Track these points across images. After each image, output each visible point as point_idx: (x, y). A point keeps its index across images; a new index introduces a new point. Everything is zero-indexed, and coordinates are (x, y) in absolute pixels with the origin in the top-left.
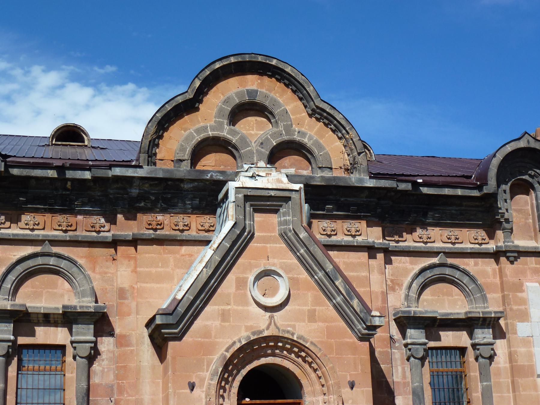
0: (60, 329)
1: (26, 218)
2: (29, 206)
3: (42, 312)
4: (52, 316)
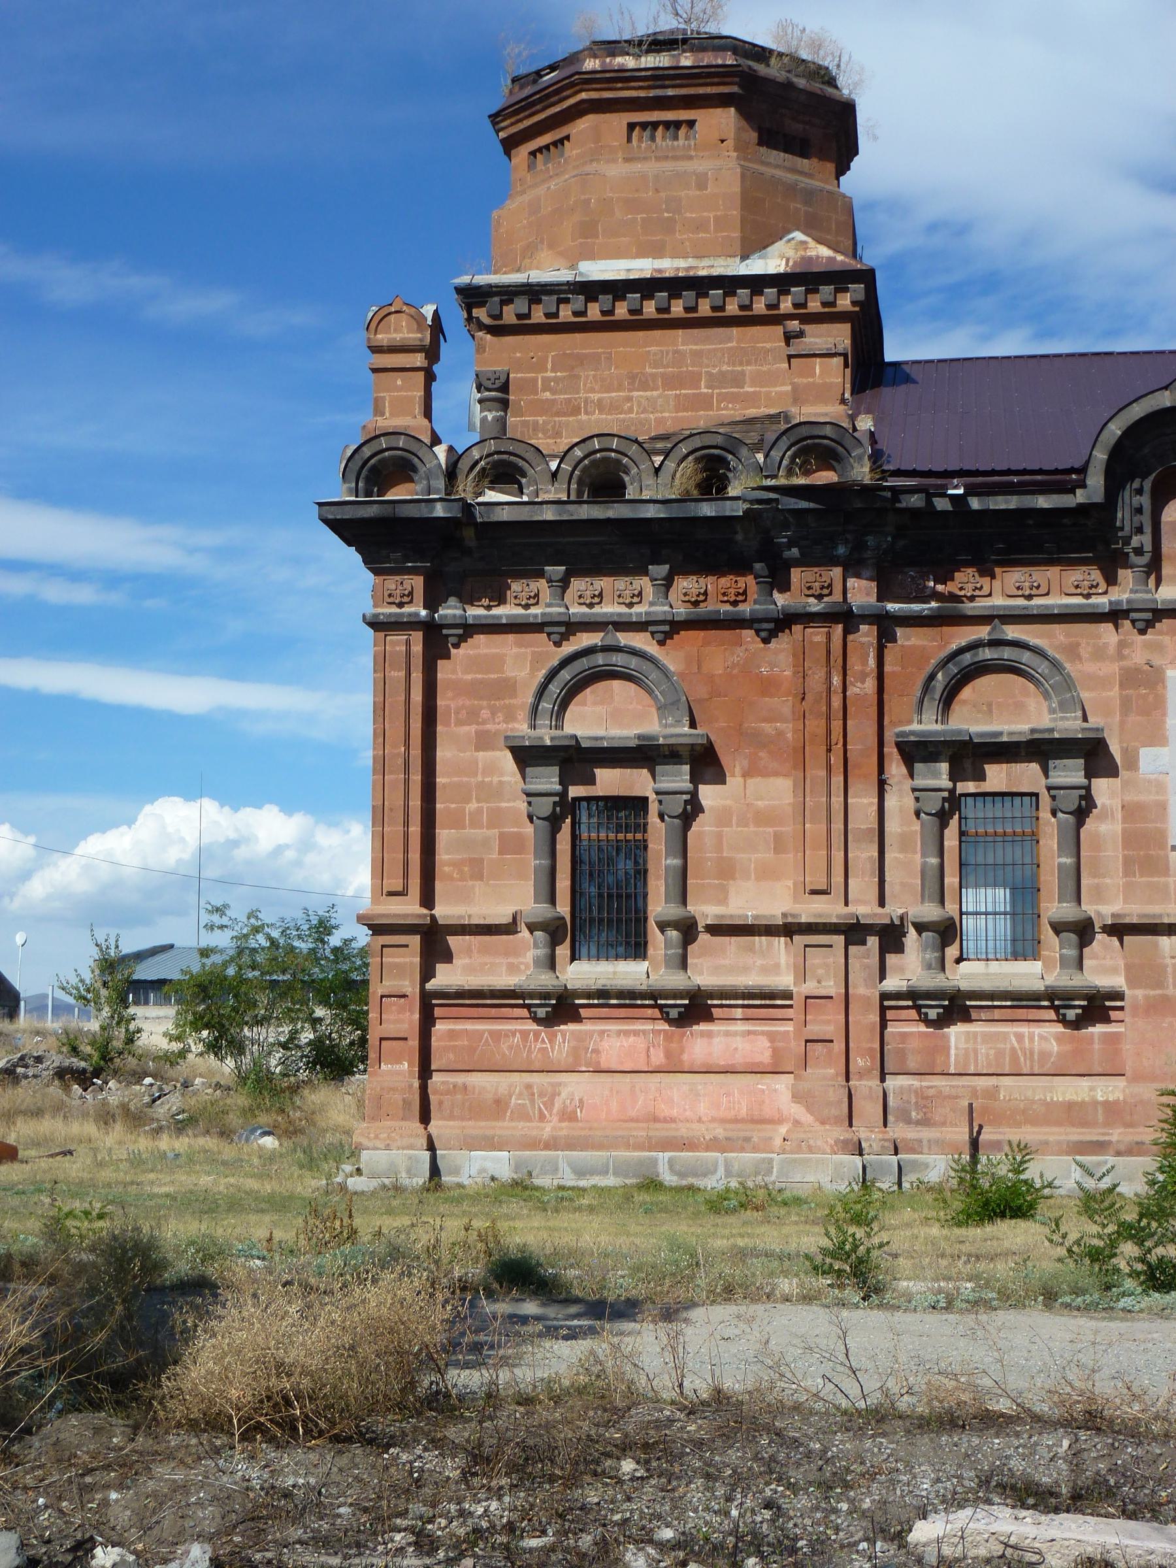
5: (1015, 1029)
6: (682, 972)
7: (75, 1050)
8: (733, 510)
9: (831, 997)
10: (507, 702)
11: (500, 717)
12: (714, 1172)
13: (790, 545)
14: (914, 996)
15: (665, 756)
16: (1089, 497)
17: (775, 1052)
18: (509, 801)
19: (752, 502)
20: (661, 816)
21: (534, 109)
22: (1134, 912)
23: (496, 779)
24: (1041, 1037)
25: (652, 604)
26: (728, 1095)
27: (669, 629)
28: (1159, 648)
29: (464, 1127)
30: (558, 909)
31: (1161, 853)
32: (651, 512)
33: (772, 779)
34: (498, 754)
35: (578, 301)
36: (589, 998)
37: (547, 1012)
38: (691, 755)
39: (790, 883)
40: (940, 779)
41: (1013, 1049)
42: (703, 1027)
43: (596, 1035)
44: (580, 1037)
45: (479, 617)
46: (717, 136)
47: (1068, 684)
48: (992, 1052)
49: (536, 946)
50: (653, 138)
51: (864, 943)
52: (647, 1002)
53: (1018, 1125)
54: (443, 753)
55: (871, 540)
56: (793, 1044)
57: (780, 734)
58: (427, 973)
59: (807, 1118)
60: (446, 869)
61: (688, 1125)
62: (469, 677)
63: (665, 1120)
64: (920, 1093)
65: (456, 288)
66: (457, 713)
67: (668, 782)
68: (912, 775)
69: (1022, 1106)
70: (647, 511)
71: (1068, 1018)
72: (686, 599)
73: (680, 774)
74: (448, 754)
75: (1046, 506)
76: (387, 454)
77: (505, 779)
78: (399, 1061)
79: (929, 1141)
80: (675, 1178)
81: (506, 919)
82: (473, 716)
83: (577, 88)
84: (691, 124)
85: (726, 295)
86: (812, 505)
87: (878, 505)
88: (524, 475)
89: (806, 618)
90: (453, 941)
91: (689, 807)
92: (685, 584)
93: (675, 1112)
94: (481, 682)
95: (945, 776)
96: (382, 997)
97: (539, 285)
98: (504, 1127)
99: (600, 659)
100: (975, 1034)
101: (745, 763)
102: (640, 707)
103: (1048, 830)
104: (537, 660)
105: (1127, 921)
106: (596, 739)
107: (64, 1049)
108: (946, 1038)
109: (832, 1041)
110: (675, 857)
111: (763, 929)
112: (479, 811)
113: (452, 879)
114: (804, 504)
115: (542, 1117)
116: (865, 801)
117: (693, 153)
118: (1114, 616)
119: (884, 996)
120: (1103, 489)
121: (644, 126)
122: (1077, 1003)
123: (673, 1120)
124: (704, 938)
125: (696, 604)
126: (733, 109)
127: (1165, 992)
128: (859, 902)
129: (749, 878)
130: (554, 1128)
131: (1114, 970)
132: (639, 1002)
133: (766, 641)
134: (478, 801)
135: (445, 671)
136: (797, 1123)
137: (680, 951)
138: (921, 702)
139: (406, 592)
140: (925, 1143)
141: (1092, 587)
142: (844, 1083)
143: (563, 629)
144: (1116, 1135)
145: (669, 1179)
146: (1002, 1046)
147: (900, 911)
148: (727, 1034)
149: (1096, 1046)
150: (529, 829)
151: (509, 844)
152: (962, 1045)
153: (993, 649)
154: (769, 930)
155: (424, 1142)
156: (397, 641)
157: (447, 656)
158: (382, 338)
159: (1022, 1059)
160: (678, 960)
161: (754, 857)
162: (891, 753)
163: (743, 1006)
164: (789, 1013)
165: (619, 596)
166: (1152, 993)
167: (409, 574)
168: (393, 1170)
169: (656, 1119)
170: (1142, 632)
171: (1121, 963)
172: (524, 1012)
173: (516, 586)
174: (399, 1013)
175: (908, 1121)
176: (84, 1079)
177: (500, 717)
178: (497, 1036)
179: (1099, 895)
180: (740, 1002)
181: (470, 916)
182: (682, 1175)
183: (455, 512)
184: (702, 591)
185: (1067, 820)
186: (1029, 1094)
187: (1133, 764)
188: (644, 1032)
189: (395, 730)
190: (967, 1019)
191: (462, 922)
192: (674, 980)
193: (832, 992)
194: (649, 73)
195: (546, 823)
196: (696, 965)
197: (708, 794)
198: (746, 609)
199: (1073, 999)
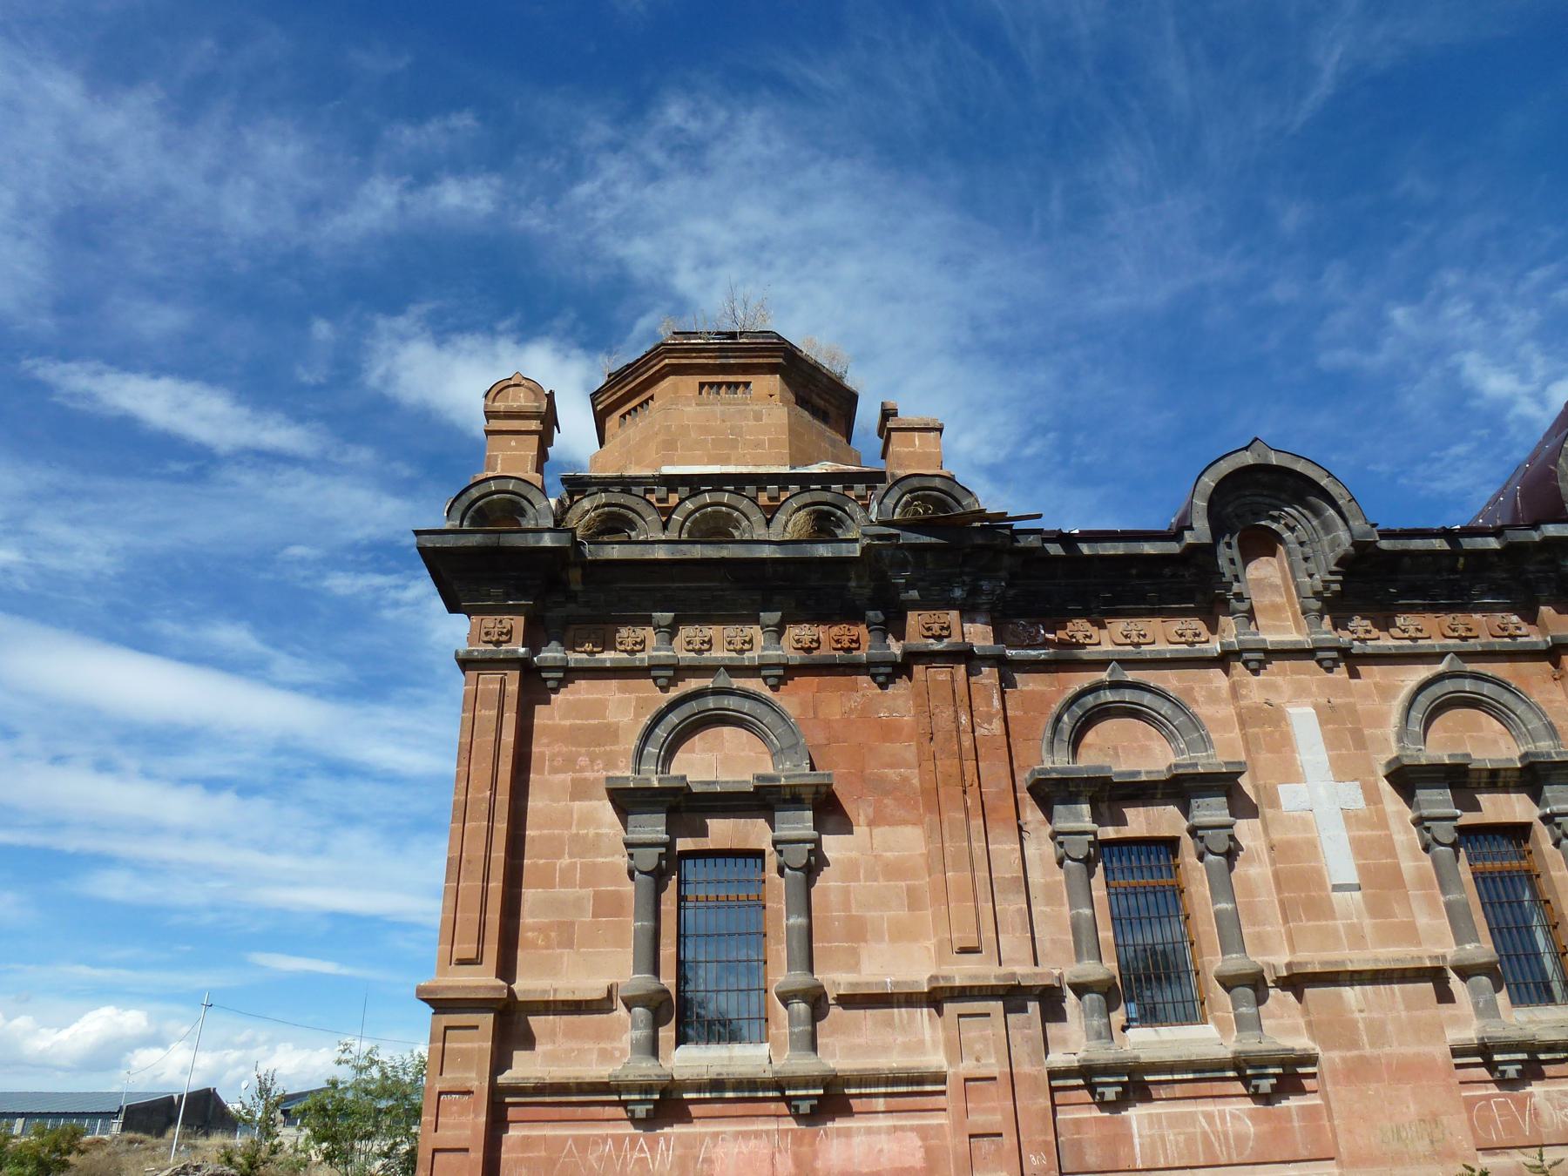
0: (1513, 796)
1: (1400, 621)
2: (1401, 602)
3: (1489, 767)
4: (1503, 773)
5: (1200, 1108)
8: (849, 552)
9: (994, 1079)
10: (608, 748)
11: (600, 764)
13: (909, 586)
14: (1088, 1074)
15: (785, 801)
16: (1198, 539)
17: (929, 1152)
18: (606, 856)
19: (873, 537)
20: (781, 872)
21: (627, 380)
22: (1314, 959)
23: (592, 832)
24: (1233, 1116)
25: (764, 649)
27: (787, 673)
28: (1273, 687)
30: (662, 982)
32: (767, 552)
33: (900, 829)
34: (595, 803)
35: (661, 491)
36: (699, 1091)
39: (931, 943)
40: (1083, 821)
41: (1205, 1135)
42: (839, 1123)
44: (684, 1141)
45: (581, 659)
46: (766, 392)
47: (1195, 722)
48: (1182, 1138)
49: (635, 1026)
50: (718, 393)
51: (1024, 1009)
52: (770, 1094)
54: (536, 803)
55: (985, 585)
56: (950, 1141)
57: (905, 780)
58: (500, 1062)
60: (530, 934)
62: (567, 723)
65: (562, 479)
67: (790, 829)
68: (1049, 817)
70: (762, 552)
71: (1261, 1091)
72: (799, 646)
73: (803, 821)
74: (540, 804)
75: (1152, 552)
76: (495, 496)
77: (603, 831)
81: (599, 994)
82: (569, 763)
83: (662, 356)
84: (747, 385)
85: (780, 489)
86: (933, 540)
87: (998, 541)
88: (633, 530)
89: (929, 657)
90: (536, 1022)
91: (813, 858)
92: (797, 631)
94: (580, 728)
95: (1088, 819)
96: (440, 1093)
97: (630, 477)
99: (711, 702)
100: (1159, 1116)
101: (870, 811)
102: (752, 754)
103: (1197, 875)
104: (641, 705)
105: (1309, 969)
108: (1126, 1123)
109: (1000, 1135)
110: (799, 916)
111: (902, 999)
116: (1007, 847)
117: (749, 402)
118: (1223, 660)
119: (1053, 1074)
120: (1209, 532)
121: (711, 385)
122: (1271, 1071)
124: (835, 1011)
125: (809, 650)
126: (778, 376)
127: (1362, 1052)
131: (1295, 1030)
132: (760, 1094)
133: (883, 686)
134: (571, 856)
137: (809, 1028)
138: (1052, 743)
139: (505, 630)
141: (1196, 635)
143: (671, 673)
146: (1193, 1130)
147: (1056, 972)
148: (869, 1131)
150: (629, 888)
151: (606, 905)
152: (1146, 1132)
153: (1113, 692)
154: (909, 1000)
157: (548, 702)
158: (500, 405)
159: (1217, 1145)
160: (807, 1039)
161: (886, 914)
162: (1024, 798)
163: (886, 1095)
165: (730, 643)
167: (509, 614)
170: (1255, 672)
171: (1302, 1022)
172: (620, 1112)
174: (461, 1115)
177: (600, 764)
178: (583, 1144)
179: (1262, 943)
180: (882, 1090)
181: (555, 991)
183: (562, 541)
184: (815, 638)
185: (1219, 862)
187: (1274, 803)
188: (767, 1132)
189: (482, 771)
190: (1147, 1098)
191: (546, 998)
193: (995, 1072)
195: (650, 878)
196: (826, 1045)
197: (832, 845)
198: (862, 655)
199: (1266, 1067)
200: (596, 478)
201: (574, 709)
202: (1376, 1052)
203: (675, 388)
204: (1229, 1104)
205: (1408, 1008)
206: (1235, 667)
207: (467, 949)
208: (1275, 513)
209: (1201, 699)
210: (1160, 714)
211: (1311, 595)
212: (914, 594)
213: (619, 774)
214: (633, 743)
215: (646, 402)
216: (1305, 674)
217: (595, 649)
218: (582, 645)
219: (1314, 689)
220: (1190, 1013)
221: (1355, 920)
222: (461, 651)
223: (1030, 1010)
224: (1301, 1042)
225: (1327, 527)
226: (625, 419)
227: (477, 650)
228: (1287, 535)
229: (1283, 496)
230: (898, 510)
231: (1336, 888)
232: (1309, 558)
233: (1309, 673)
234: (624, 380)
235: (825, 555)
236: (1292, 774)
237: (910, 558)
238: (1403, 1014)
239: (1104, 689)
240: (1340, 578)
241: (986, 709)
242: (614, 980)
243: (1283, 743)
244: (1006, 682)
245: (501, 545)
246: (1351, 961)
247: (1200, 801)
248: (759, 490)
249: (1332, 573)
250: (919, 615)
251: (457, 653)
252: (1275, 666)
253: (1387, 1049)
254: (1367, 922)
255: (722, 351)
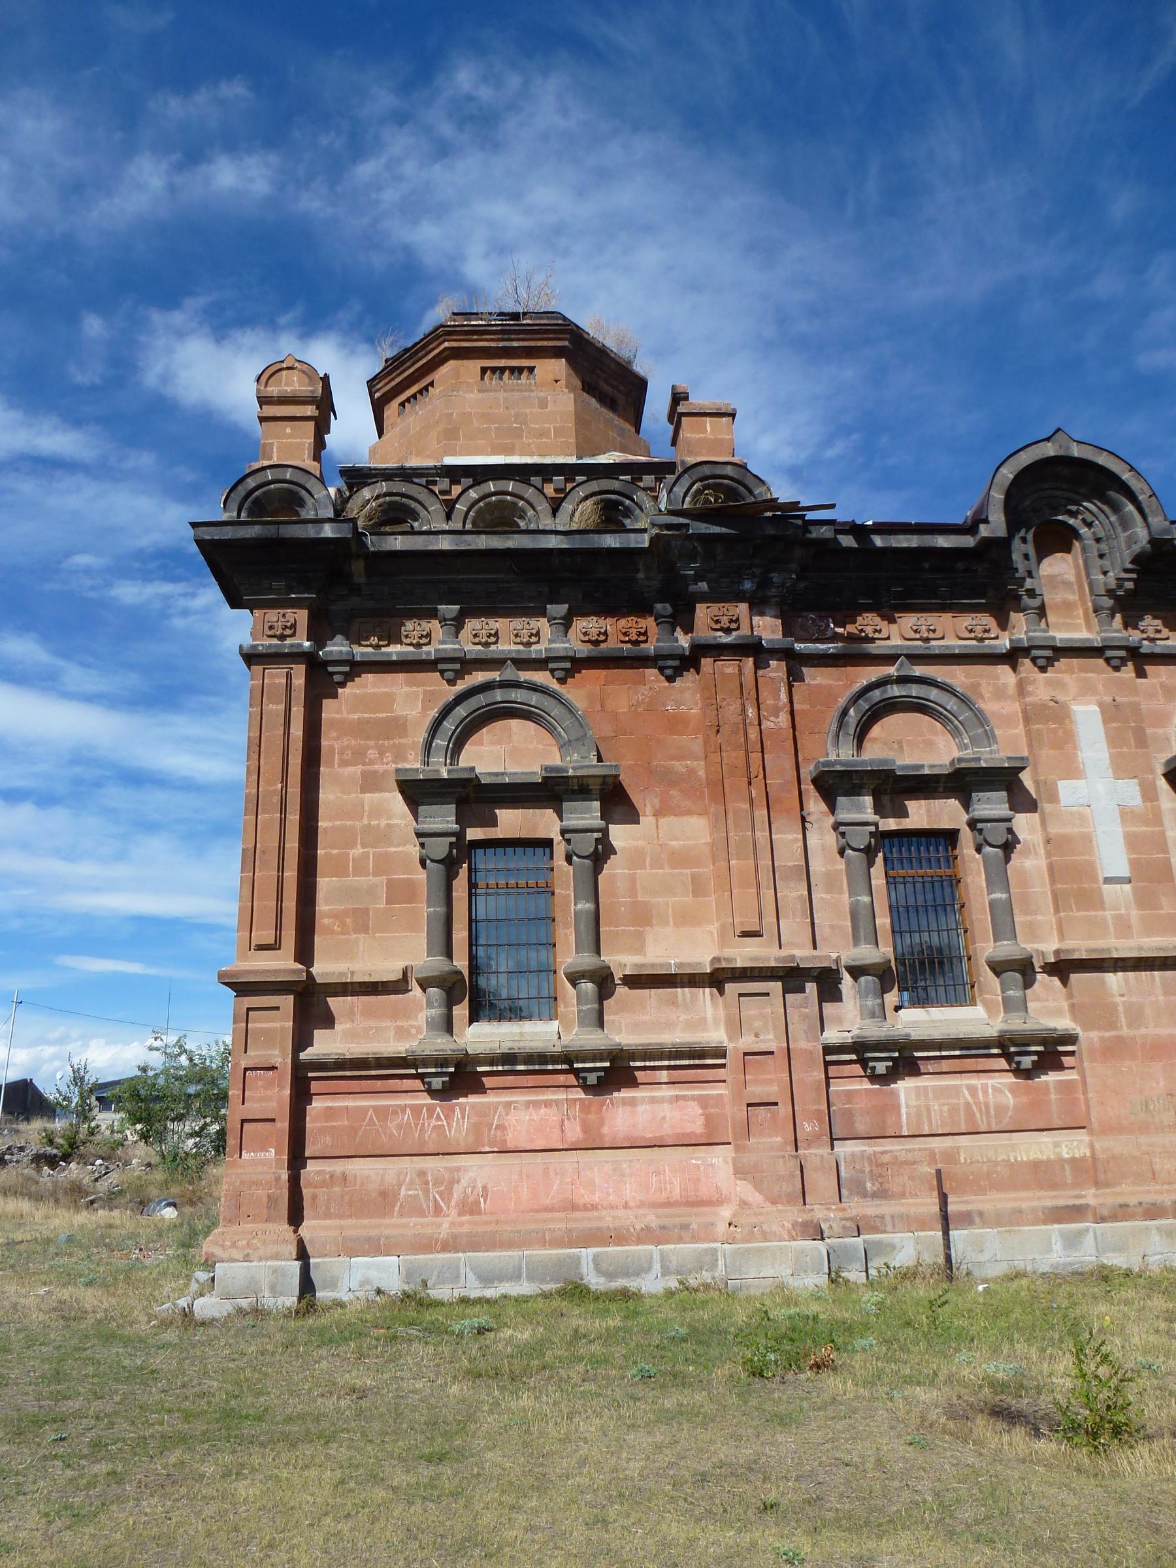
5: (965, 1082)
6: (600, 1031)
7: (51, 1142)
8: (638, 542)
9: (772, 1053)
10: (396, 741)
11: (389, 756)
12: (649, 1268)
13: (698, 578)
14: (861, 1050)
15: (573, 792)
16: (993, 532)
17: (709, 1120)
18: (399, 845)
19: (661, 527)
20: (569, 859)
22: (1081, 946)
23: (383, 822)
24: (995, 1089)
25: (551, 641)
26: (657, 1173)
27: (575, 665)
29: (342, 1228)
31: (1094, 886)
32: (553, 542)
33: (685, 818)
34: (386, 795)
35: (444, 483)
36: (492, 1065)
37: (443, 1082)
38: (602, 790)
39: (714, 928)
40: (866, 813)
41: (968, 1105)
42: (625, 1093)
43: (500, 1109)
45: (367, 654)
46: (551, 377)
47: (980, 718)
48: (946, 1108)
49: (430, 1005)
50: (501, 379)
52: (559, 1067)
53: (982, 1191)
54: (327, 795)
55: (776, 577)
56: (728, 1110)
57: (691, 772)
58: (302, 1040)
59: (755, 1198)
60: (326, 921)
61: (613, 1212)
62: (356, 716)
63: (586, 1208)
64: (873, 1160)
66: (341, 753)
67: (578, 819)
68: (832, 809)
69: (985, 1169)
71: (1023, 1066)
72: (586, 638)
73: (589, 810)
74: (331, 797)
75: (946, 545)
76: (272, 486)
78: (264, 1149)
79: (892, 1217)
80: (602, 1280)
81: (395, 976)
82: (359, 756)
85: (566, 481)
86: (724, 530)
89: (717, 650)
90: (334, 1003)
91: (600, 847)
92: (585, 624)
93: (596, 1198)
94: (368, 721)
95: (870, 810)
96: (246, 1069)
97: (411, 468)
98: (392, 1225)
99: (498, 695)
100: (926, 1088)
101: (657, 802)
102: (541, 747)
103: (974, 866)
104: (428, 698)
105: (1076, 956)
106: (496, 774)
107: (45, 1140)
108: (895, 1094)
109: (776, 1104)
110: (587, 901)
111: (686, 979)
112: (365, 856)
113: (332, 932)
114: (716, 529)
115: (438, 1211)
116: (790, 837)
117: (533, 388)
118: (1012, 657)
119: (828, 1050)
120: (1004, 524)
121: (494, 370)
122: (1033, 1048)
123: (594, 1207)
124: (621, 991)
125: (596, 643)
127: (1120, 1033)
128: (792, 945)
129: (665, 923)
130: (453, 1224)
131: (1058, 1013)
132: (550, 1067)
133: (670, 679)
134: (363, 846)
135: (330, 710)
136: (744, 1204)
137: (596, 1006)
140: (888, 1219)
141: (986, 631)
142: (794, 1153)
144: (1090, 1196)
145: (595, 1282)
146: (955, 1101)
147: (834, 956)
148: (653, 1100)
149: (1053, 1097)
150: (421, 875)
151: (399, 892)
152: (913, 1103)
154: (693, 980)
155: (293, 1250)
156: (276, 676)
157: (335, 696)
158: (273, 390)
159: (978, 1115)
160: (594, 1017)
162: (807, 790)
163: (669, 1068)
164: (720, 1073)
165: (517, 636)
166: (1107, 1034)
168: (252, 1289)
169: (574, 1207)
170: (1043, 669)
171: (1065, 1005)
172: (417, 1084)
173: (409, 625)
175: (864, 1194)
176: (52, 1162)
177: (389, 756)
178: (382, 1113)
179: (1033, 932)
180: (666, 1063)
181: (352, 973)
182: (611, 1276)
183: (343, 532)
184: (603, 630)
185: (996, 852)
186: (991, 1154)
187: (1054, 798)
188: (557, 1102)
189: (271, 763)
191: (344, 980)
192: (592, 1039)
193: (772, 1047)
194: (499, 328)
195: (441, 866)
196: (613, 1022)
197: (619, 834)
198: (650, 647)
199: (1029, 1045)
200: (376, 469)
201: (362, 703)
202: (1132, 1033)
203: (456, 373)
204: (992, 1078)
205: (1166, 994)
206: (1023, 664)
207: (268, 937)
208: (1074, 508)
209: (987, 695)
210: (946, 709)
211: (1103, 593)
212: (703, 586)
213: (408, 766)
214: (421, 736)
215: (426, 388)
216: (1092, 672)
217: (381, 643)
218: (368, 639)
219: (1100, 687)
220: (961, 994)
221: (1123, 912)
222: (245, 645)
223: (807, 990)
224: (1064, 1024)
225: (1125, 524)
226: (404, 407)
227: (262, 645)
228: (1084, 531)
229: (1082, 490)
230: (688, 499)
231: (1108, 880)
232: (1104, 555)
233: (1097, 672)
234: (402, 365)
235: (613, 546)
236: (1073, 771)
237: (699, 548)
238: (1161, 998)
239: (892, 684)
240: (1134, 576)
241: (772, 702)
242: (407, 963)
243: (1066, 740)
244: (794, 676)
245: (280, 536)
246: (1116, 950)
247: (981, 794)
248: (545, 481)
249: (1126, 571)
250: (708, 607)
251: (241, 647)
252: (1063, 663)
253: (1143, 1031)
254: (1135, 913)
255: (505, 333)
